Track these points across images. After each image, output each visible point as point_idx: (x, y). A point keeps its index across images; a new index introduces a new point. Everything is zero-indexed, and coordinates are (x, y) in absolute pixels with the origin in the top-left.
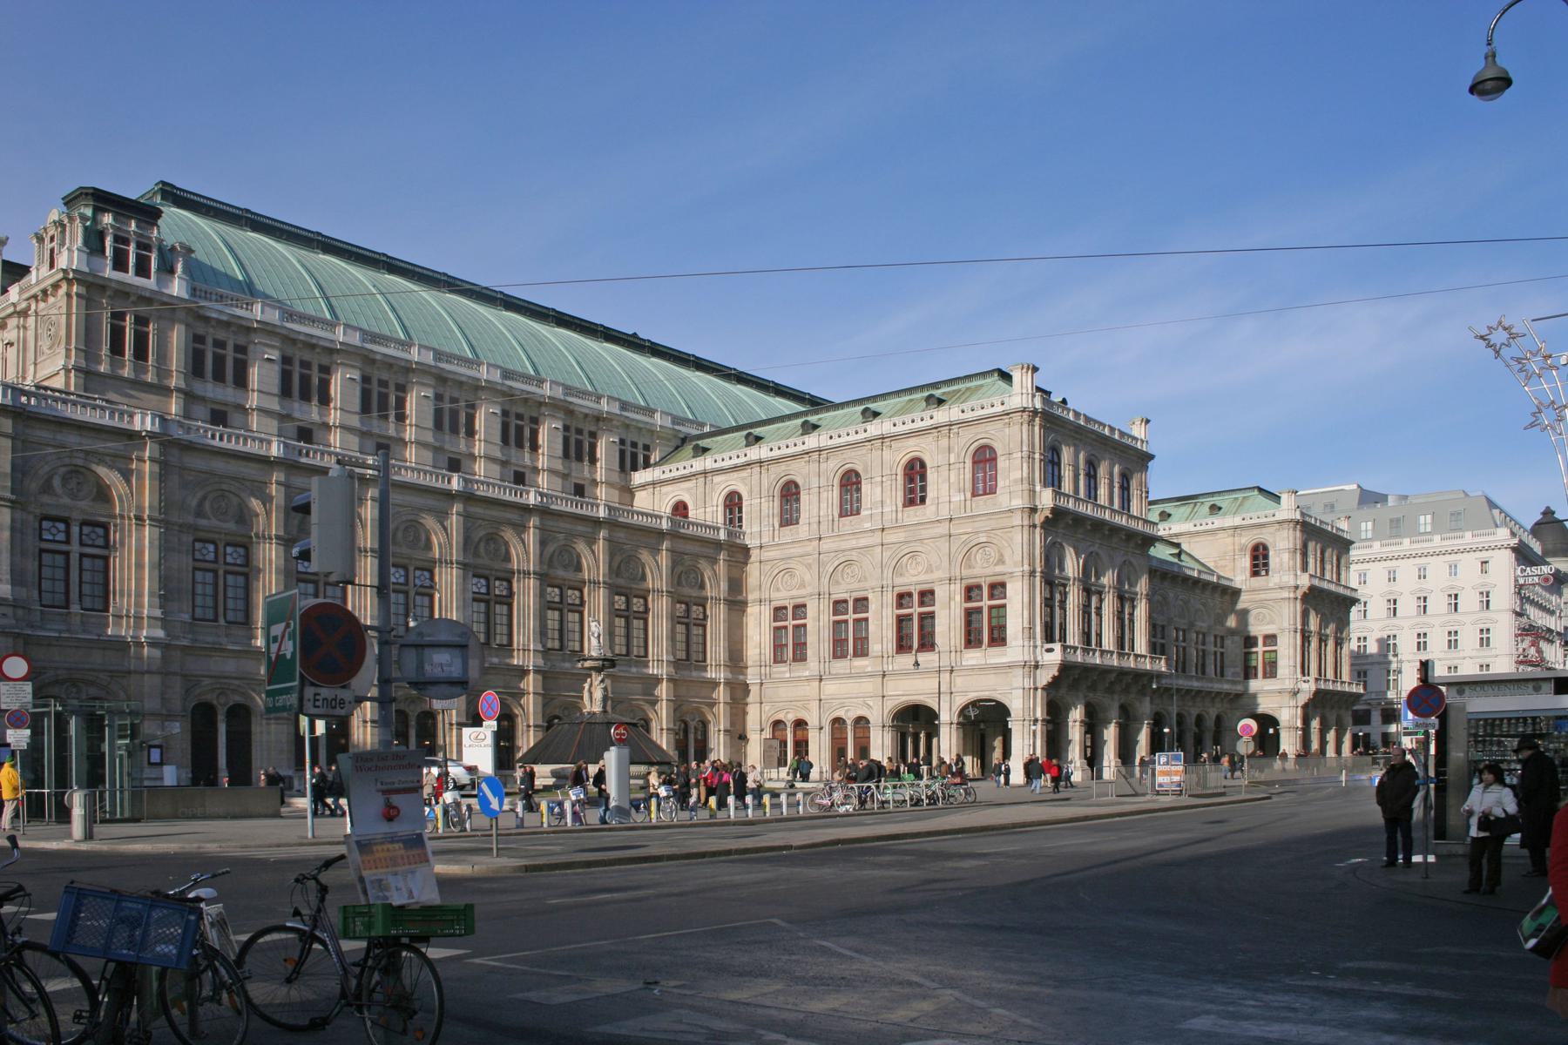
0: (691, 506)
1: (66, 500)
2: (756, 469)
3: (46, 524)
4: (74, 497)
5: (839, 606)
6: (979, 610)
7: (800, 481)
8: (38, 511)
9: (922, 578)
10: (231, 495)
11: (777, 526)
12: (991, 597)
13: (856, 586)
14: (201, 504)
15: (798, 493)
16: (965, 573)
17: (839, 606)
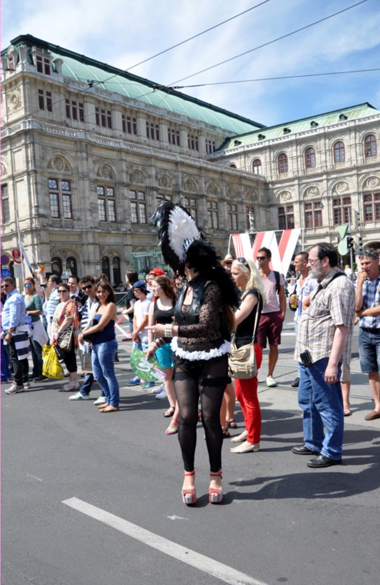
0: (238, 167)
1: (56, 171)
2: (268, 150)
3: (50, 181)
4: (58, 169)
5: (307, 205)
6: (370, 205)
7: (288, 155)
8: (48, 176)
9: (345, 193)
10: (107, 166)
11: (278, 173)
12: (376, 199)
13: (315, 197)
14: (98, 171)
15: (287, 159)
16: (365, 190)
17: (307, 205)
